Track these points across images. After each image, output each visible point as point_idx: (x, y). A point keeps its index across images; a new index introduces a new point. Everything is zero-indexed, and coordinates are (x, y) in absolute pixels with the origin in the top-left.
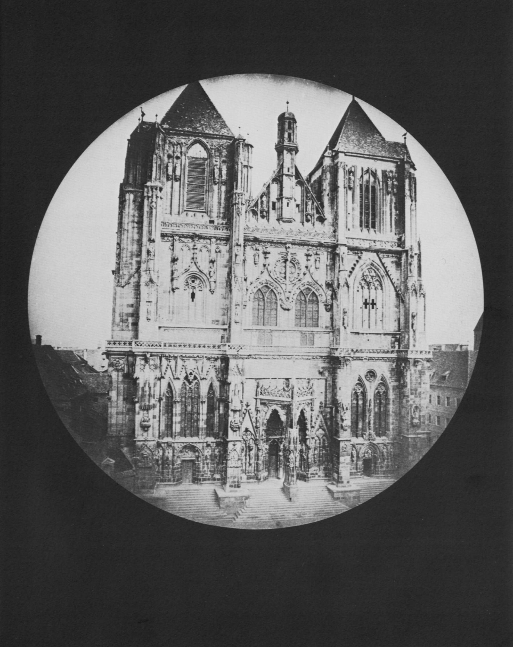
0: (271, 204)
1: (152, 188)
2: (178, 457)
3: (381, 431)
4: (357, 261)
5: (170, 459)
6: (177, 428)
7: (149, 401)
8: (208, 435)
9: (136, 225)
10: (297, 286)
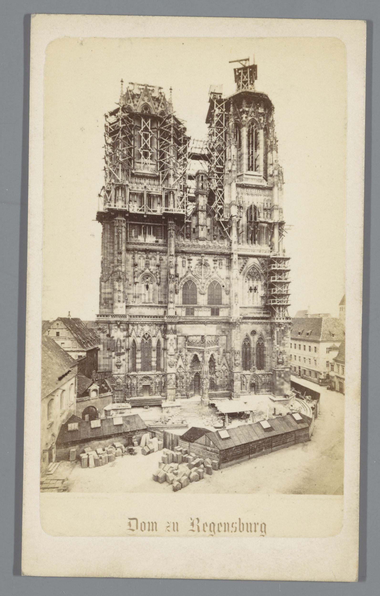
0: (192, 230)
1: (119, 220)
2: (140, 383)
3: (261, 366)
5: (135, 384)
6: (139, 366)
7: (120, 351)
8: (157, 370)
9: (111, 244)
10: (209, 280)
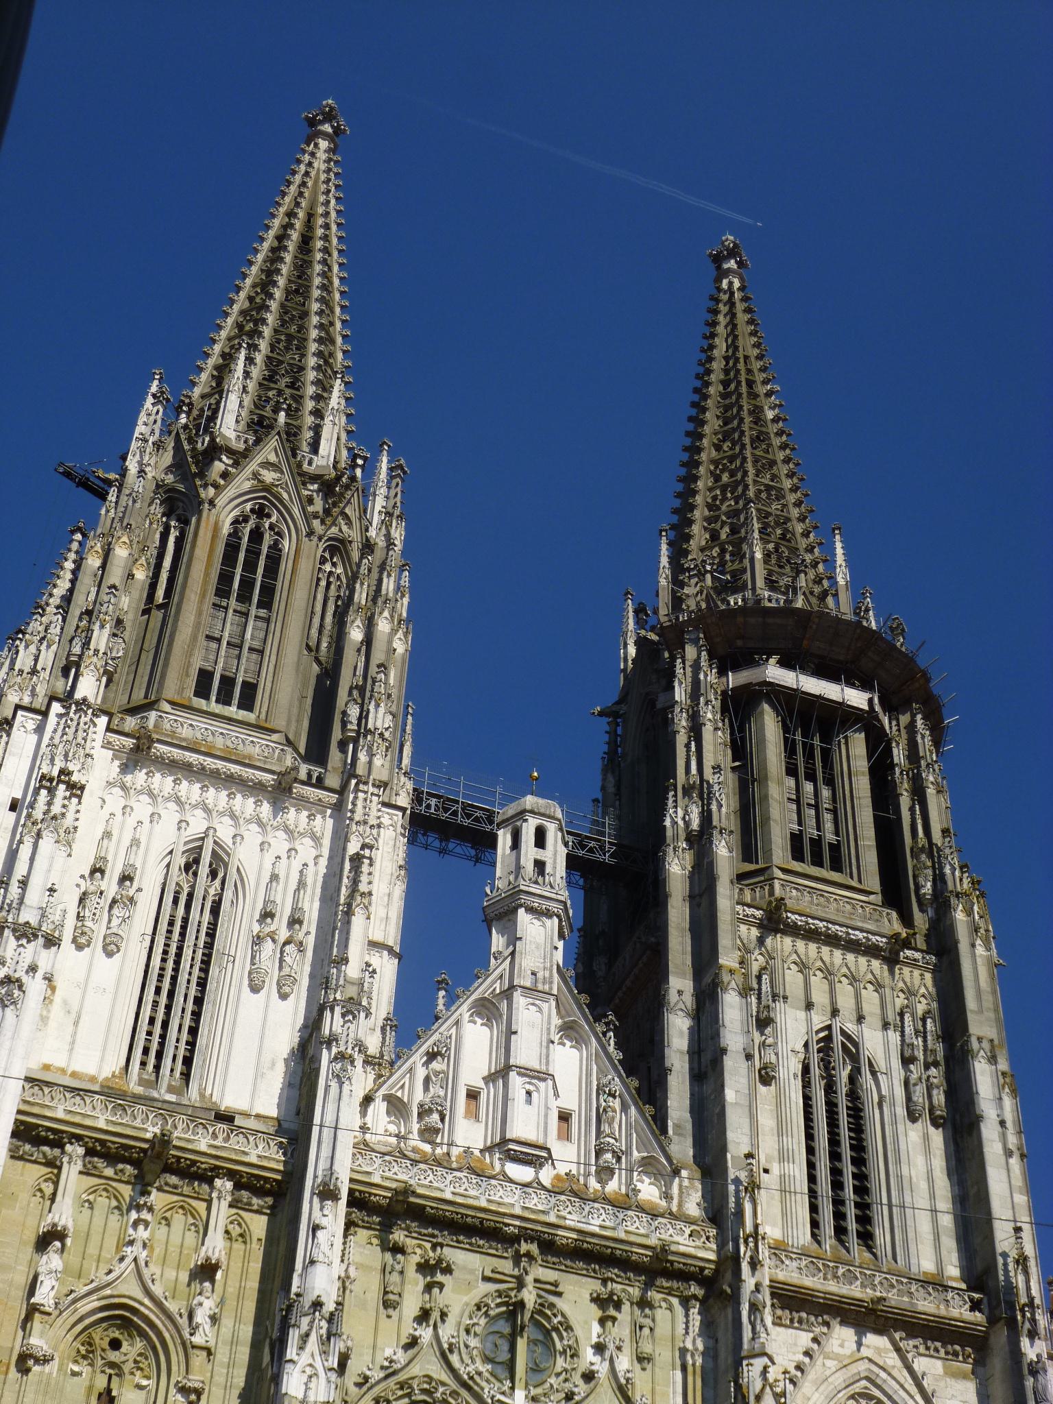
4: (807, 1353)
